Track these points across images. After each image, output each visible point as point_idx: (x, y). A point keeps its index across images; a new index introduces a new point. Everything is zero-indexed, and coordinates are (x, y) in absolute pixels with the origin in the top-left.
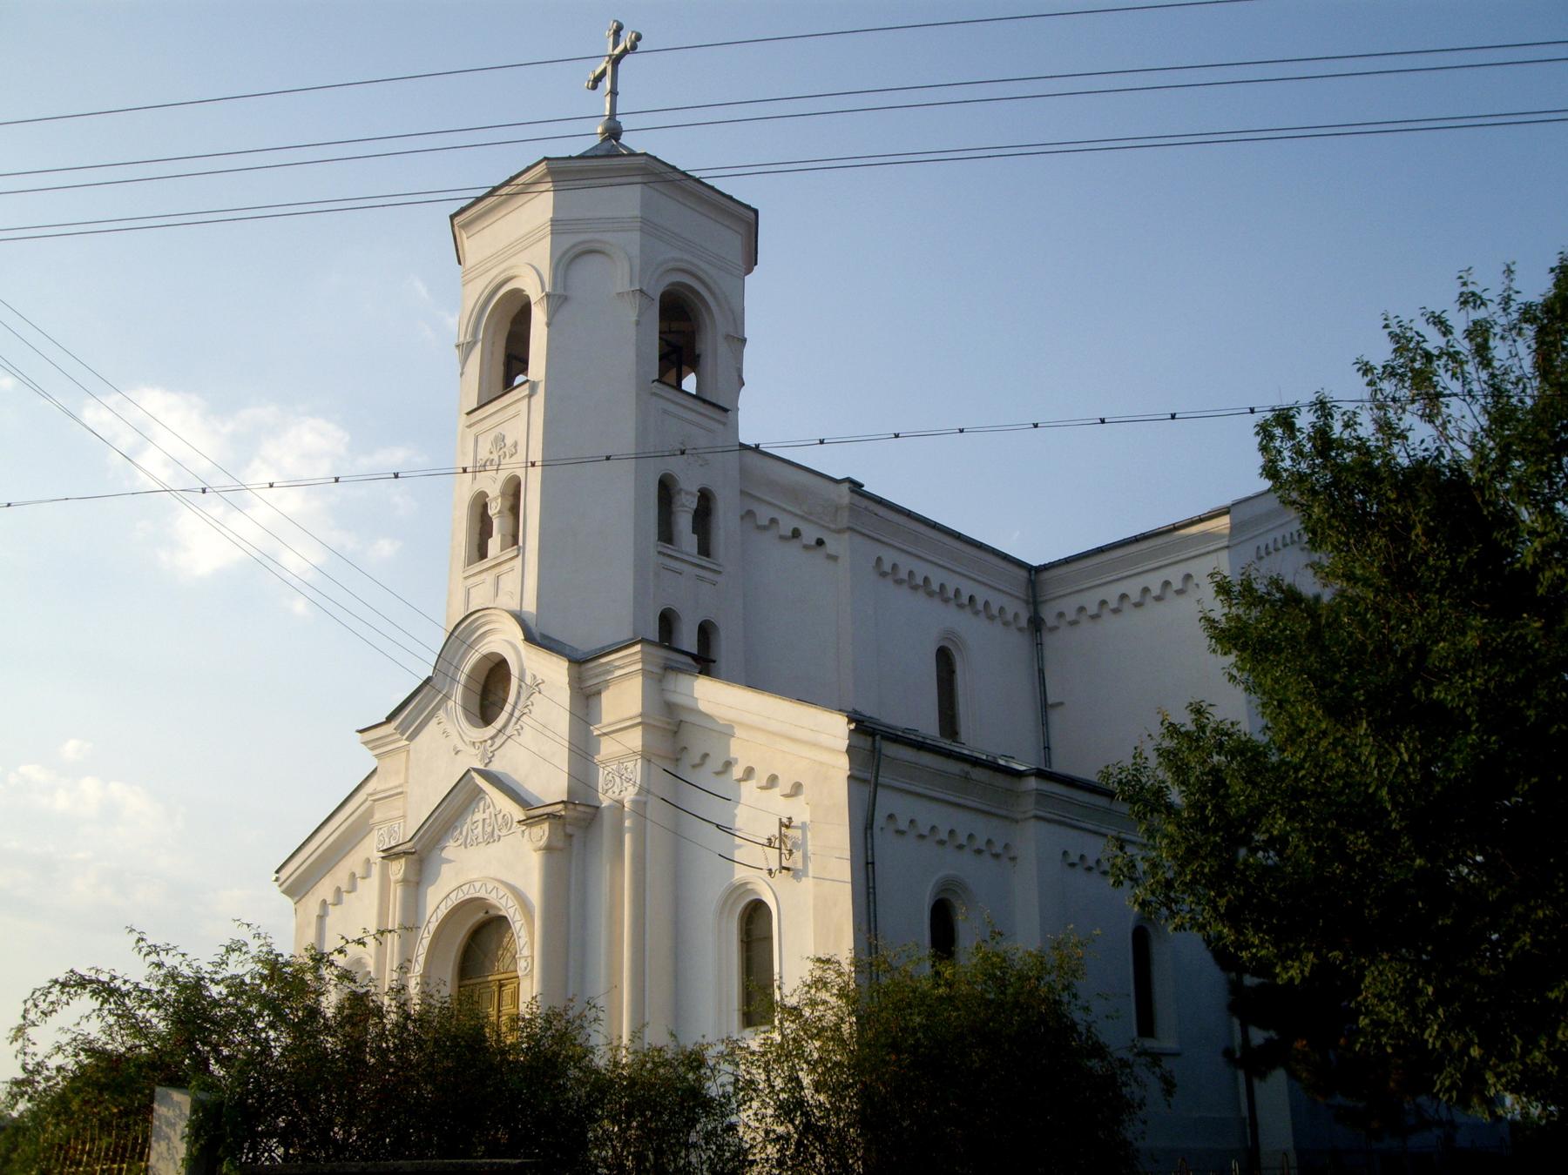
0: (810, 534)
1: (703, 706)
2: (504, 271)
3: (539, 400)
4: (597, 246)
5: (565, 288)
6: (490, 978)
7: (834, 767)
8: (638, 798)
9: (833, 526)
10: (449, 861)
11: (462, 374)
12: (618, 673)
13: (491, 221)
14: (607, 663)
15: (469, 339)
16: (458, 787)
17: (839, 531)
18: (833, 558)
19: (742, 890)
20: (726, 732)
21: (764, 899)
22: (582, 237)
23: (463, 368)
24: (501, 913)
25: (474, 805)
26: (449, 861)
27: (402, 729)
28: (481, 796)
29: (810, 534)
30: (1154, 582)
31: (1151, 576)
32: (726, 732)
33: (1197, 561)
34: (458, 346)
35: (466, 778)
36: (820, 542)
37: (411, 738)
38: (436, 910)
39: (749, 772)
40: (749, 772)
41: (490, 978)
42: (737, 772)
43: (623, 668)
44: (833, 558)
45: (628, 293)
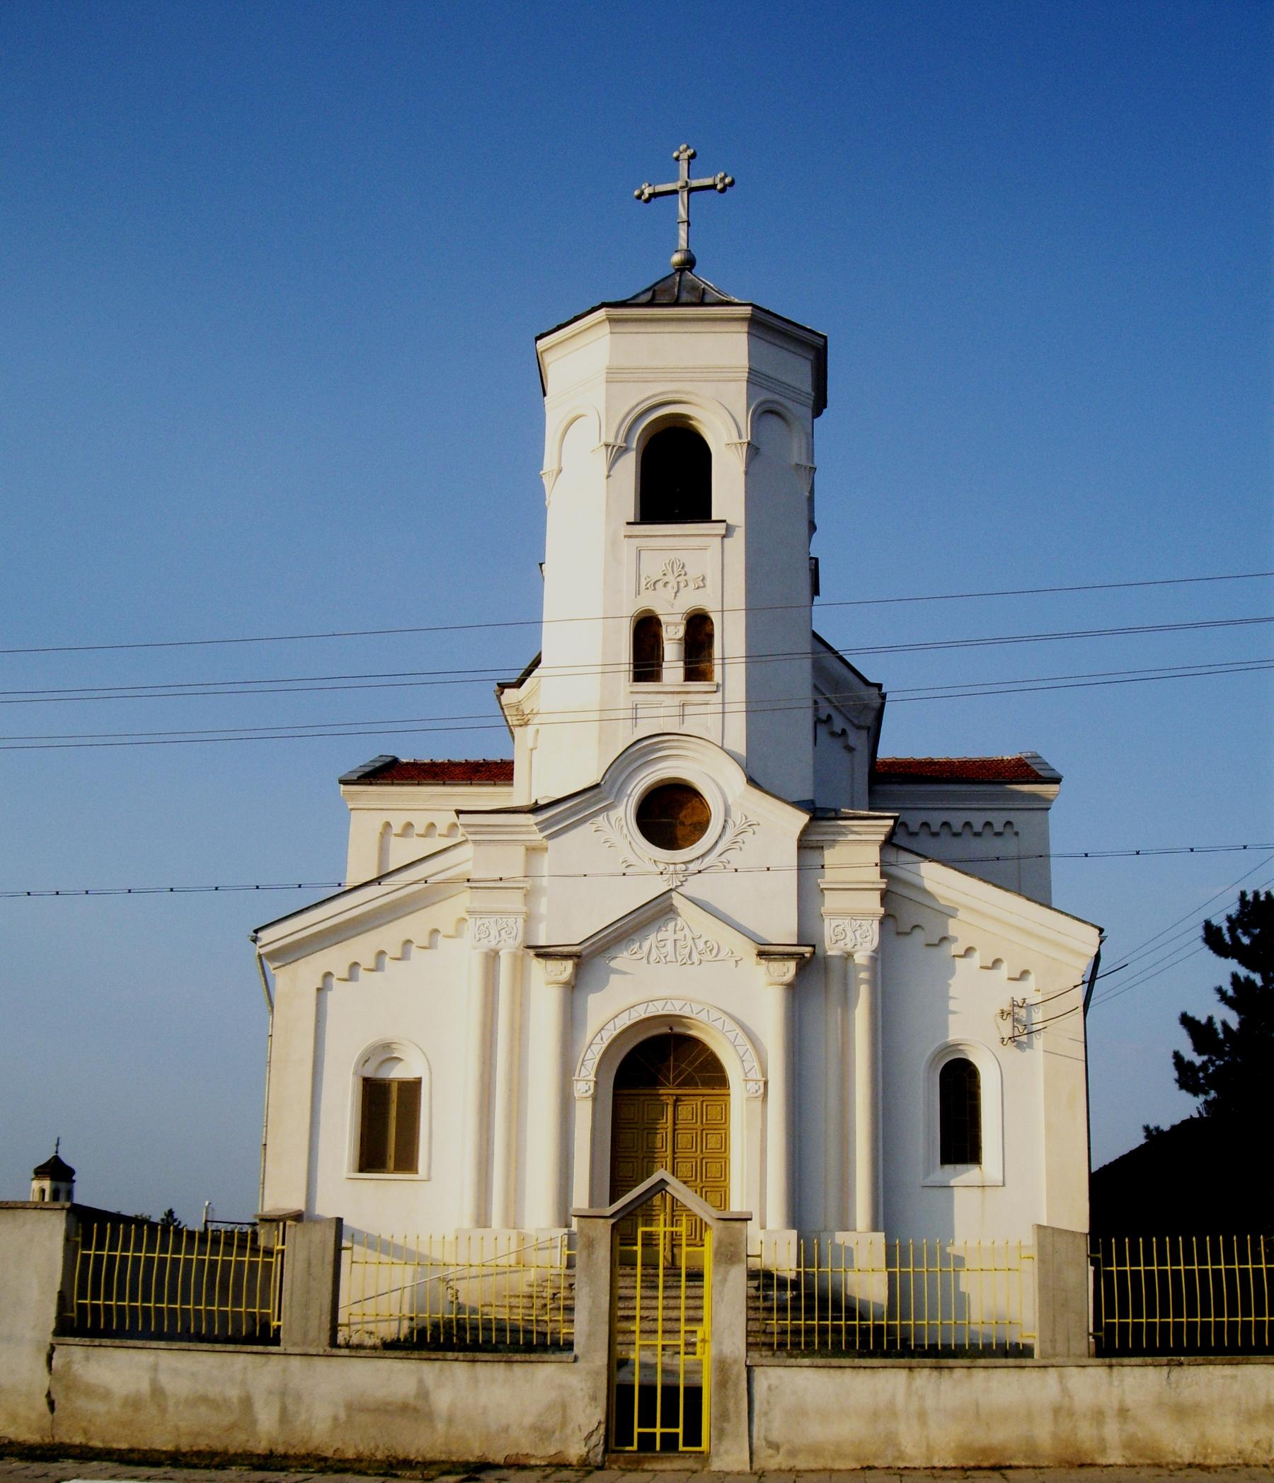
0: (838, 724)
1: (929, 885)
2: (677, 392)
3: (737, 544)
4: (778, 408)
5: (811, 456)
6: (661, 1092)
7: (1067, 965)
8: (874, 955)
9: (856, 722)
10: (954, 1013)
11: (608, 476)
12: (851, 837)
13: (653, 330)
14: (844, 826)
15: (620, 442)
16: (654, 903)
17: (859, 728)
18: (850, 749)
19: (954, 1048)
20: (948, 913)
21: (971, 1059)
22: (776, 397)
23: (610, 470)
24: (693, 1033)
25: (661, 922)
26: (954, 1013)
27: (543, 826)
28: (671, 915)
29: (838, 724)
30: (978, 820)
31: (995, 814)
32: (948, 913)
33: (1018, 813)
34: (607, 445)
35: (665, 897)
36: (844, 732)
37: (550, 837)
38: (614, 1018)
39: (969, 951)
40: (969, 951)
41: (661, 1092)
42: (956, 948)
43: (860, 834)
44: (850, 749)
45: (805, 468)
